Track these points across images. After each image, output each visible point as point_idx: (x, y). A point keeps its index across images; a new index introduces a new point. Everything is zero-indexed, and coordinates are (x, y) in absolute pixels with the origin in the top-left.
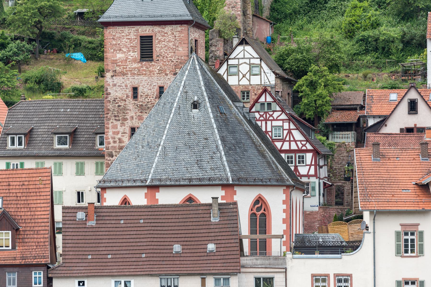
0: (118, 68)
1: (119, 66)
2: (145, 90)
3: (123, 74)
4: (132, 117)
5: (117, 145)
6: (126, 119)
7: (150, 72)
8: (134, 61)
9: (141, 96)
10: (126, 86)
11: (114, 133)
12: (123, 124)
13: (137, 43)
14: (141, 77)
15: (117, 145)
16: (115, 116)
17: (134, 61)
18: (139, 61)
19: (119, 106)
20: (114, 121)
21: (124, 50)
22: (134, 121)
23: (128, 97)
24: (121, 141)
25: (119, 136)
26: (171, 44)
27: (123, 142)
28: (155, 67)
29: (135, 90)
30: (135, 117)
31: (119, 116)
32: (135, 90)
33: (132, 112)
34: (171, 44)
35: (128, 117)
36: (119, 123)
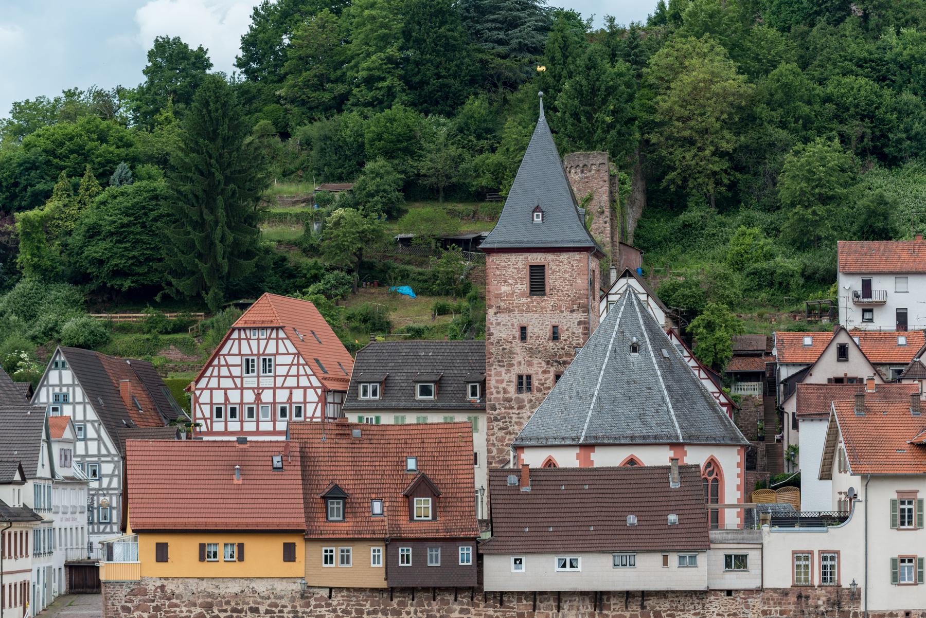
0: (502, 304)
1: (504, 301)
2: (536, 330)
3: (510, 311)
4: (520, 363)
5: (501, 396)
6: (512, 365)
7: (542, 308)
8: (523, 295)
10: (513, 325)
11: (497, 381)
12: (508, 371)
13: (526, 273)
14: (531, 314)
16: (499, 361)
17: (523, 295)
19: (504, 349)
21: (511, 282)
22: (522, 367)
23: (514, 338)
24: (505, 391)
25: (504, 385)
27: (509, 393)
28: (548, 302)
29: (523, 329)
32: (523, 329)
33: (520, 356)
34: (567, 275)
35: (515, 363)
36: (503, 370)
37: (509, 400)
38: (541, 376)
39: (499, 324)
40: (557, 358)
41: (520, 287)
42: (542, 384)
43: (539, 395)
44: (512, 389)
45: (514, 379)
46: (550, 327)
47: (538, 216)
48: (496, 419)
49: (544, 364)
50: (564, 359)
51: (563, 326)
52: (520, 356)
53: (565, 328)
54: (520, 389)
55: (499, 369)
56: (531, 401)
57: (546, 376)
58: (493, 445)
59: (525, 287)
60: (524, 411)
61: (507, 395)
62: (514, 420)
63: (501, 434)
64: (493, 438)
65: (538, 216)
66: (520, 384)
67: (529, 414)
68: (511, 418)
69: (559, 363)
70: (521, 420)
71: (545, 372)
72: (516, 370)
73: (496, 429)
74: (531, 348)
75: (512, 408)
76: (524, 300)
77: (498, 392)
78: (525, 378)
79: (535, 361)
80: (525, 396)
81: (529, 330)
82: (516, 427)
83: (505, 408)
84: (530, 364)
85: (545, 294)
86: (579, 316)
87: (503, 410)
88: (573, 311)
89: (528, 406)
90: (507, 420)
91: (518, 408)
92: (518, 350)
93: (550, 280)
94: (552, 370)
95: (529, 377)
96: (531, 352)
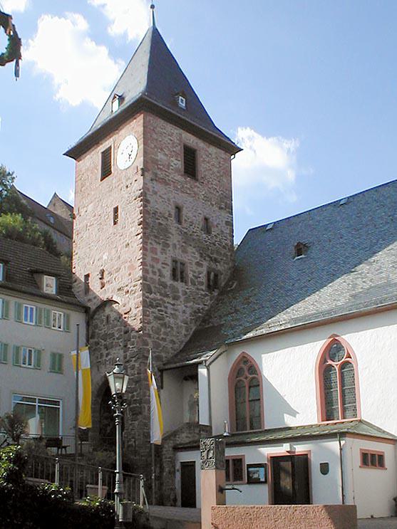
2: (190, 214)
4: (175, 245)
6: (168, 245)
8: (177, 170)
9: (185, 220)
10: (169, 200)
11: (153, 259)
12: (163, 251)
13: (180, 149)
15: (156, 278)
16: (156, 237)
17: (177, 170)
18: (183, 173)
19: (160, 224)
20: (153, 243)
22: (177, 251)
25: (159, 266)
26: (215, 170)
27: (164, 277)
28: (202, 191)
29: (179, 209)
30: (178, 246)
31: (159, 238)
32: (179, 209)
33: (175, 238)
35: (171, 243)
36: (159, 248)
37: (164, 285)
38: (194, 267)
39: (156, 193)
40: (209, 253)
41: (176, 162)
42: (197, 277)
43: (193, 288)
44: (167, 273)
45: (169, 262)
46: (202, 217)
47: (182, 100)
48: (151, 306)
49: (197, 255)
50: (215, 256)
51: (214, 220)
52: (175, 238)
53: (215, 223)
54: (174, 276)
55: (155, 246)
56: (186, 293)
57: (200, 269)
58: (149, 336)
59: (178, 163)
60: (179, 302)
61: (163, 280)
62: (169, 311)
63: (156, 324)
64: (149, 327)
65: (182, 100)
66: (174, 270)
67: (184, 308)
68: (166, 307)
69: (211, 258)
70: (177, 313)
71: (198, 264)
72: (171, 253)
73: (151, 318)
74: (185, 233)
75: (167, 296)
76: (179, 178)
77: (154, 273)
78: (179, 265)
79: (190, 249)
80: (179, 285)
81: (184, 211)
82: (172, 320)
83: (161, 294)
84: (185, 251)
85: (197, 180)
86: (224, 214)
87: (158, 296)
88: (221, 208)
89: (182, 298)
90: (163, 309)
91: (174, 299)
92: (173, 230)
93: (202, 167)
94: (205, 264)
95: (183, 264)
96: (187, 238)
